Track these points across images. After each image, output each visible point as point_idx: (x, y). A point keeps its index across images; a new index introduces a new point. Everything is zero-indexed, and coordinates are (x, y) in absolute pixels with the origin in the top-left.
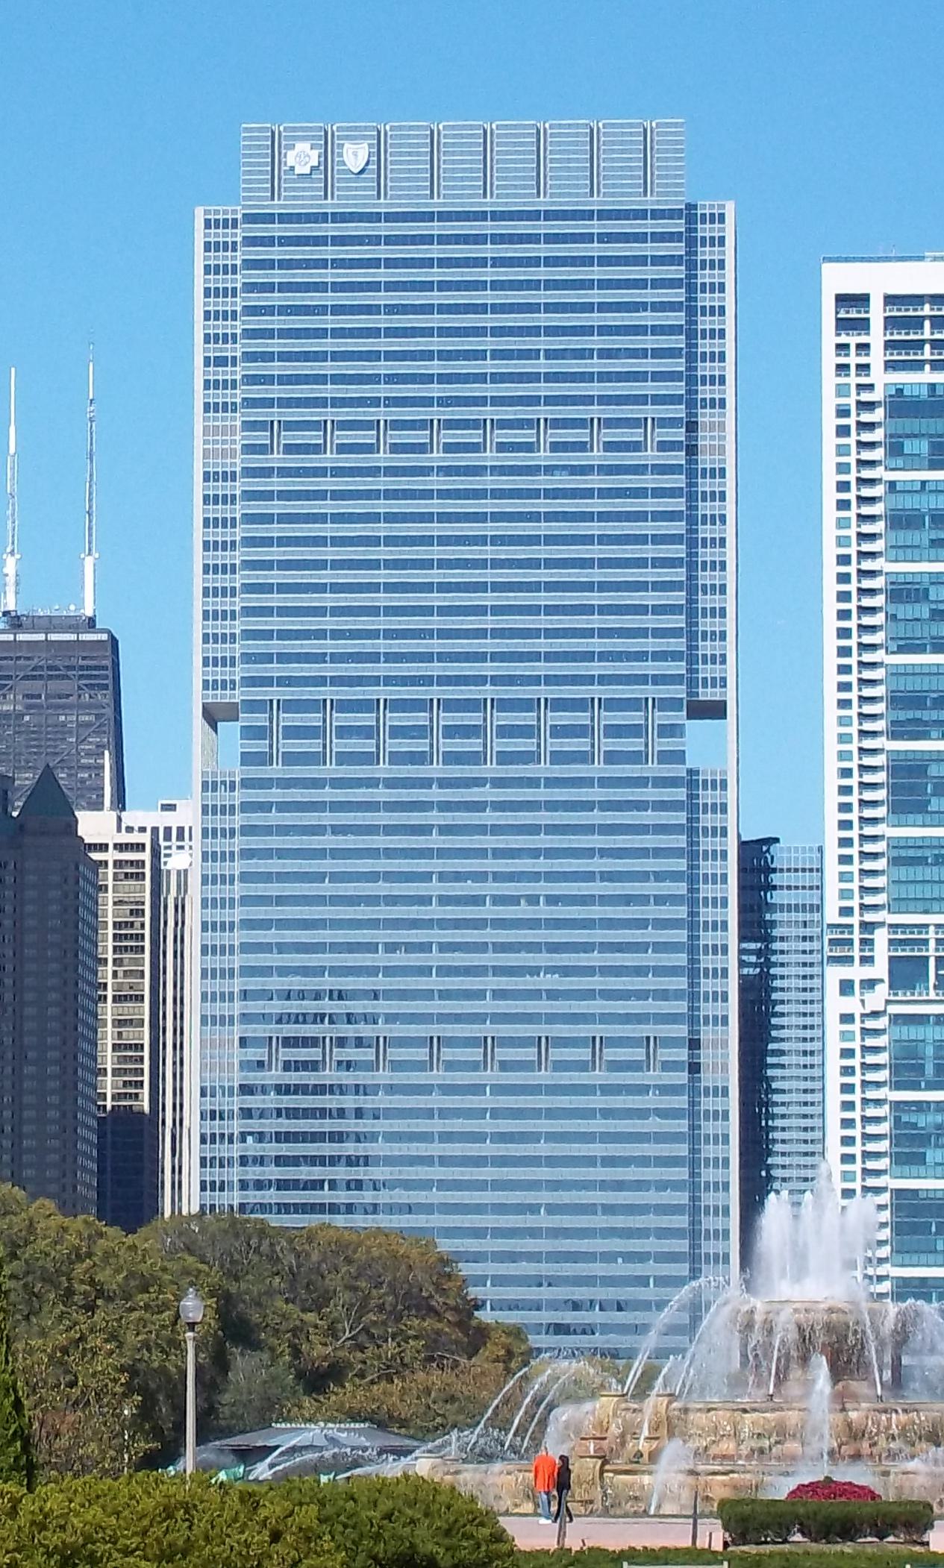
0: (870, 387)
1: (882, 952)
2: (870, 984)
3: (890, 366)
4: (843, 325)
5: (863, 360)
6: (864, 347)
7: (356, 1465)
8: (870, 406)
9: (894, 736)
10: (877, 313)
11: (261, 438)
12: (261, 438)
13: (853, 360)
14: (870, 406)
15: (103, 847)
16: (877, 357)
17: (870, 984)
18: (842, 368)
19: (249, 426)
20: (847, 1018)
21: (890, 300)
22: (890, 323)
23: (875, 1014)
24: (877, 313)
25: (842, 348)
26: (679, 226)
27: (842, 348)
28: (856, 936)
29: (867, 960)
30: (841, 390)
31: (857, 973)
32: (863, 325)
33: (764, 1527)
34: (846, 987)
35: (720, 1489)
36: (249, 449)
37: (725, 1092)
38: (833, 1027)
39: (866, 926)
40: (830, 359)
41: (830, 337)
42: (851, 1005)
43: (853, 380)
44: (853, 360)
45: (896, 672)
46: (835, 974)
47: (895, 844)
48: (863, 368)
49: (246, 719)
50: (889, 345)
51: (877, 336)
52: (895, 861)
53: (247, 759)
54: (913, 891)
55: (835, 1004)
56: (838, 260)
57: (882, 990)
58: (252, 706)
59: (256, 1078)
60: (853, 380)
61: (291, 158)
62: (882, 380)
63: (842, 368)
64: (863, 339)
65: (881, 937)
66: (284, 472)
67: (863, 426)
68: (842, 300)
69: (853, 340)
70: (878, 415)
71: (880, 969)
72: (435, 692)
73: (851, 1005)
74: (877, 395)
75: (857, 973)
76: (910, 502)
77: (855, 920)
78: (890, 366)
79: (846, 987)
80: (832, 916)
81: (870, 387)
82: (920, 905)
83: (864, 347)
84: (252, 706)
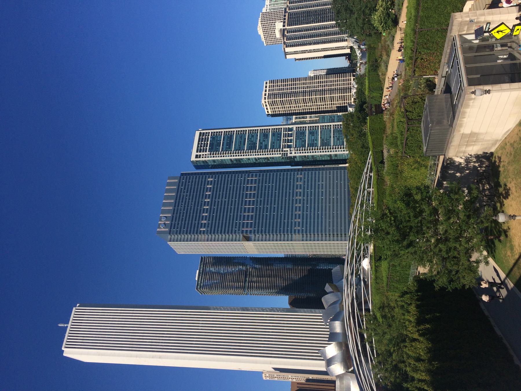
2: (290, 151)
3: (206, 152)
4: (200, 157)
10: (199, 154)
13: (204, 156)
16: (204, 153)
20: (295, 153)
21: (197, 152)
22: (200, 152)
24: (199, 154)
25: (203, 157)
31: (289, 152)
32: (200, 155)
34: (291, 153)
42: (293, 152)
48: (206, 155)
51: (201, 153)
62: (207, 153)
65: (284, 149)
71: (288, 149)
73: (293, 152)
75: (289, 152)
76: (224, 149)
77: (281, 152)
78: (206, 152)
79: (291, 153)
80: (281, 155)
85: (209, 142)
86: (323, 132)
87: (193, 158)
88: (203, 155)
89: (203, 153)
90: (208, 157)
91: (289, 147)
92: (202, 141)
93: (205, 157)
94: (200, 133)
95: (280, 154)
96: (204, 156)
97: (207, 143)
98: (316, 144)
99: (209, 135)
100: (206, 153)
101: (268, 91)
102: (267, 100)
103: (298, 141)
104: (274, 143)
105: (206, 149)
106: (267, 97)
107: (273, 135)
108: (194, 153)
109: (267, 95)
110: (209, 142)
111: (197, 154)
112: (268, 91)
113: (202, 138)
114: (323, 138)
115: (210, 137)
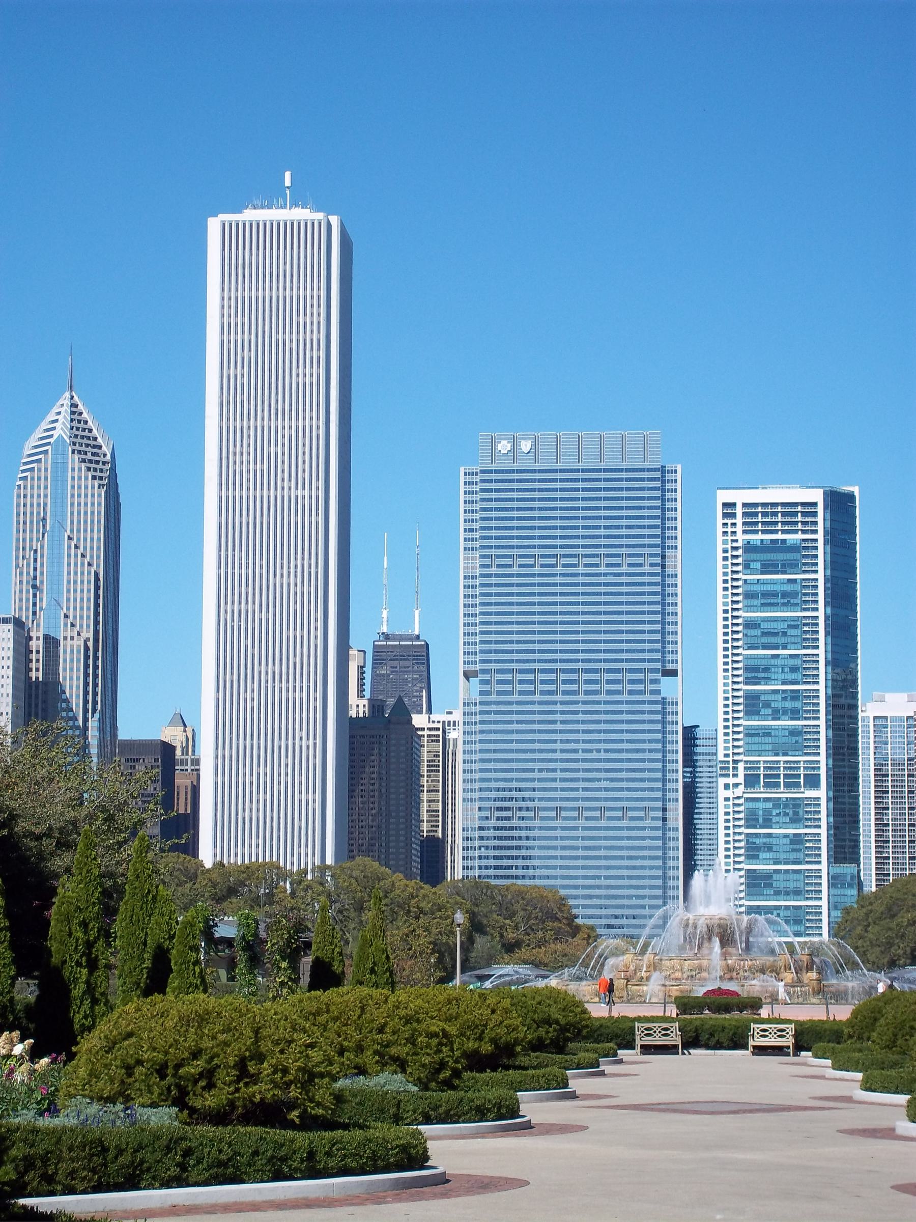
0: (737, 541)
1: (741, 772)
2: (736, 785)
3: (745, 532)
4: (725, 515)
5: (733, 530)
6: (734, 524)
7: (526, 982)
8: (736, 548)
9: (746, 683)
10: (739, 510)
11: (487, 561)
12: (487, 561)
14: (736, 548)
15: (423, 729)
16: (739, 528)
17: (736, 785)
18: (725, 533)
19: (482, 557)
20: (727, 799)
21: (745, 505)
22: (745, 514)
23: (738, 798)
24: (739, 510)
26: (658, 475)
27: (725, 525)
28: (731, 766)
29: (735, 775)
30: (725, 542)
31: (731, 780)
32: (734, 515)
33: (693, 1007)
34: (727, 786)
35: (675, 992)
36: (482, 566)
37: (677, 829)
38: (721, 803)
39: (735, 762)
40: (720, 529)
41: (720, 520)
42: (729, 794)
43: (730, 538)
44: (729, 530)
45: (747, 658)
46: (722, 781)
47: (747, 728)
48: (734, 533)
49: (481, 677)
50: (744, 523)
51: (739, 520)
52: (747, 735)
53: (482, 693)
54: (754, 747)
55: (722, 793)
56: (723, 489)
57: (742, 787)
58: (484, 671)
59: (485, 824)
60: (730, 538)
61: (499, 447)
62: (741, 538)
63: (725, 533)
64: (734, 521)
65: (741, 766)
66: (497, 575)
67: (734, 557)
68: (725, 505)
69: (729, 521)
70: (740, 552)
71: (741, 779)
72: (559, 666)
73: (729, 794)
74: (739, 544)
75: (731, 780)
76: (752, 588)
77: (730, 759)
79: (727, 786)
80: (721, 757)
81: (737, 541)
82: (757, 753)
83: (734, 524)
84: (484, 671)
85: (780, 536)
86: (796, 876)
87: (724, 496)
91: (751, 780)
92: (784, 514)
94: (815, 504)
96: (729, 530)
97: (776, 532)
98: (757, 857)
99: (804, 532)
103: (769, 805)
104: (769, 735)
107: (794, 732)
108: (740, 497)
113: (795, 514)
114: (775, 877)
115: (800, 536)
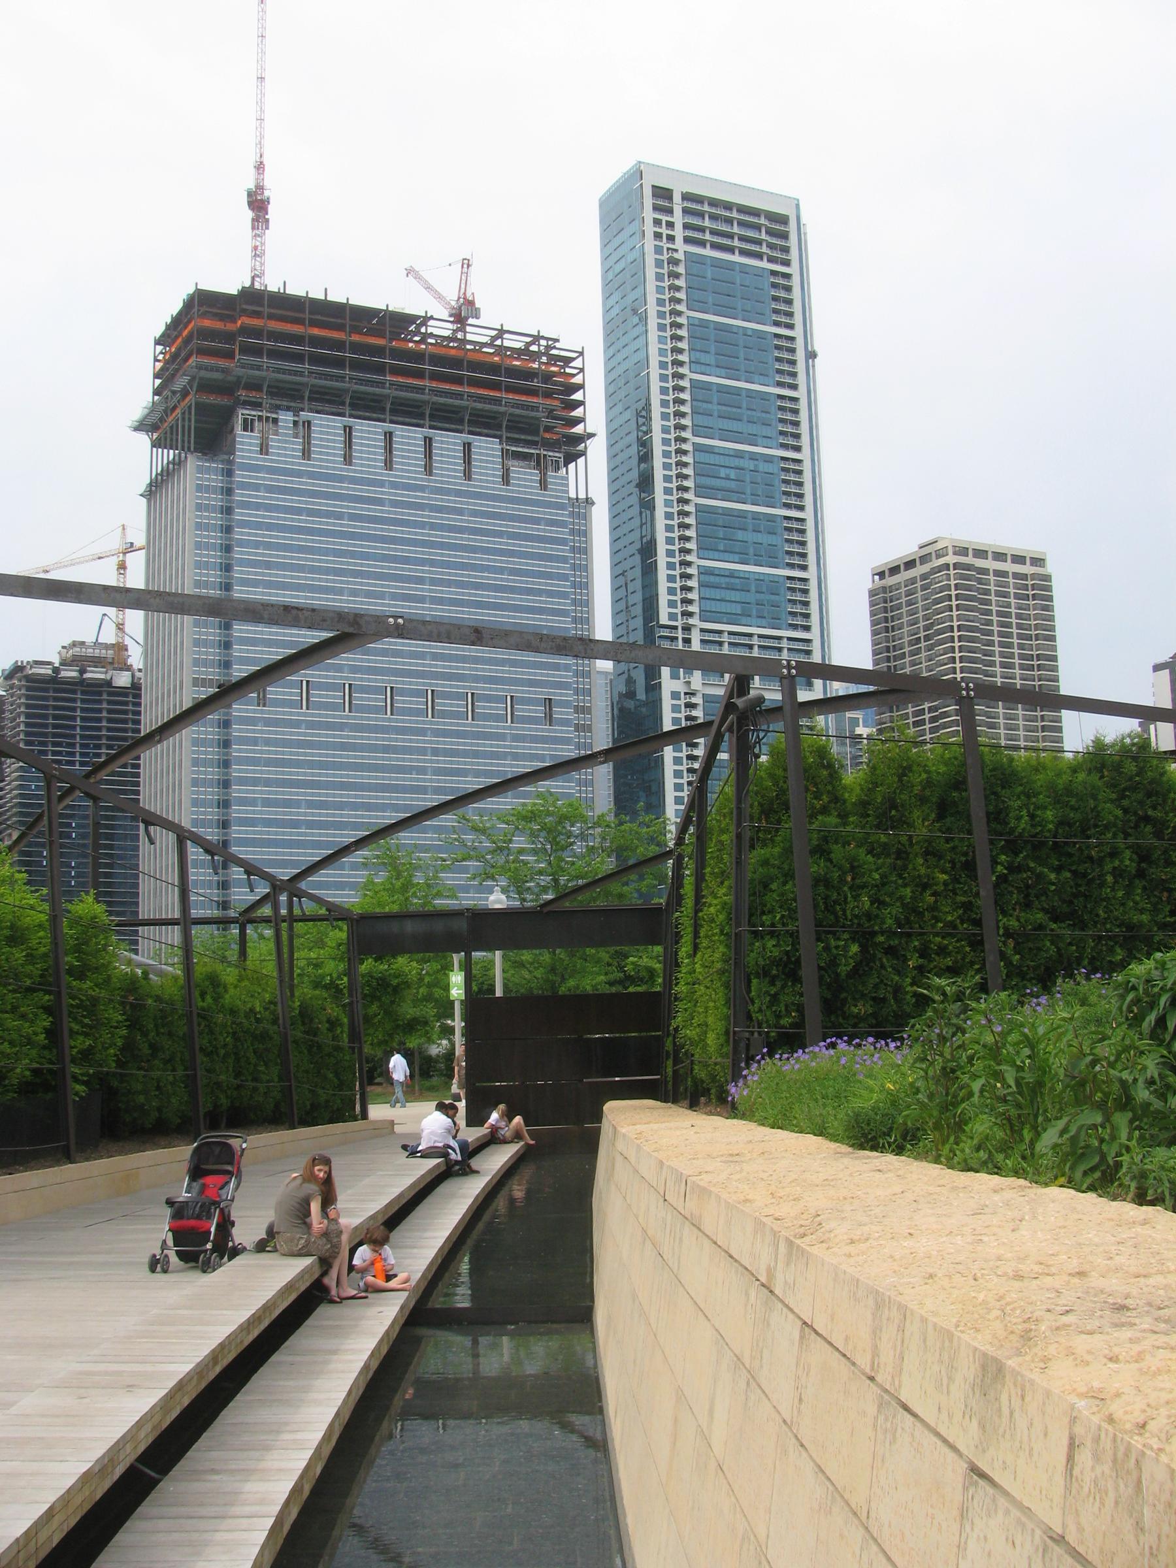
3: (687, 240)
4: (656, 208)
13: (664, 231)
16: (679, 232)
20: (675, 695)
21: (686, 197)
22: (686, 211)
25: (657, 222)
32: (670, 211)
38: (667, 703)
41: (649, 214)
48: (671, 238)
51: (678, 218)
69: (664, 218)
77: (679, 623)
88: (670, 225)
89: (679, 227)
90: (659, 250)
93: (658, 236)
95: (672, 616)
96: (664, 231)
99: (771, 260)
100: (679, 243)
101: (1000, 566)
102: (951, 559)
105: (702, 243)
106: (969, 560)
109: (980, 563)
110: (736, 258)
111: (677, 198)
112: (1000, 566)
115: (765, 264)
